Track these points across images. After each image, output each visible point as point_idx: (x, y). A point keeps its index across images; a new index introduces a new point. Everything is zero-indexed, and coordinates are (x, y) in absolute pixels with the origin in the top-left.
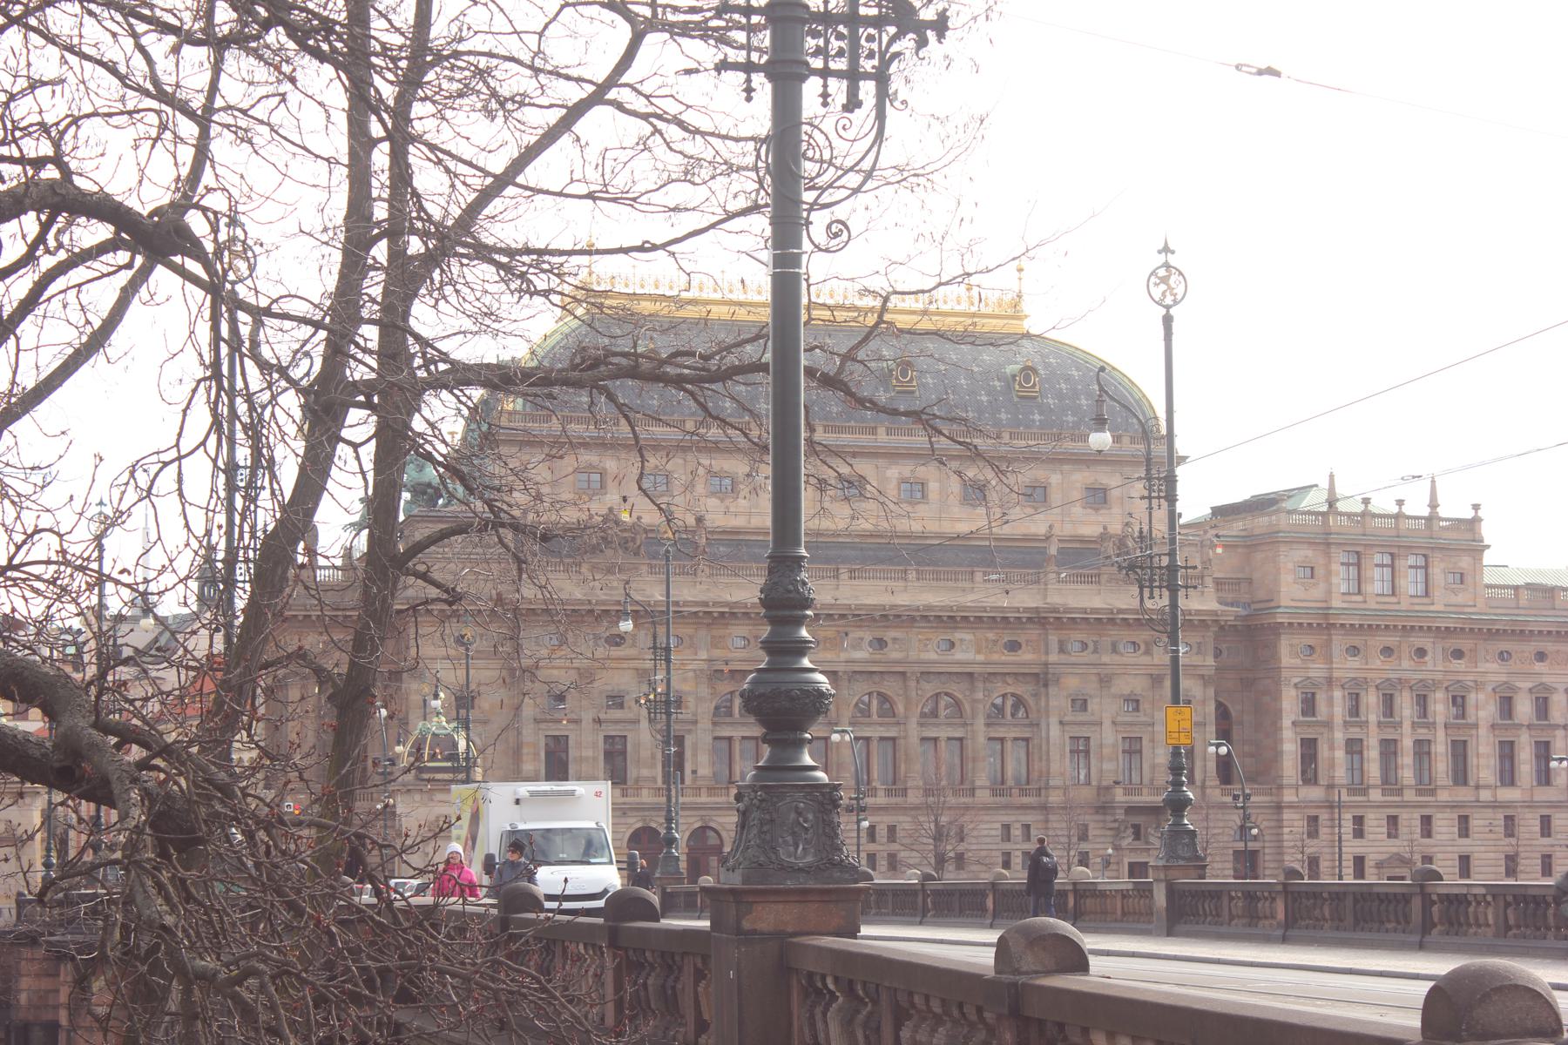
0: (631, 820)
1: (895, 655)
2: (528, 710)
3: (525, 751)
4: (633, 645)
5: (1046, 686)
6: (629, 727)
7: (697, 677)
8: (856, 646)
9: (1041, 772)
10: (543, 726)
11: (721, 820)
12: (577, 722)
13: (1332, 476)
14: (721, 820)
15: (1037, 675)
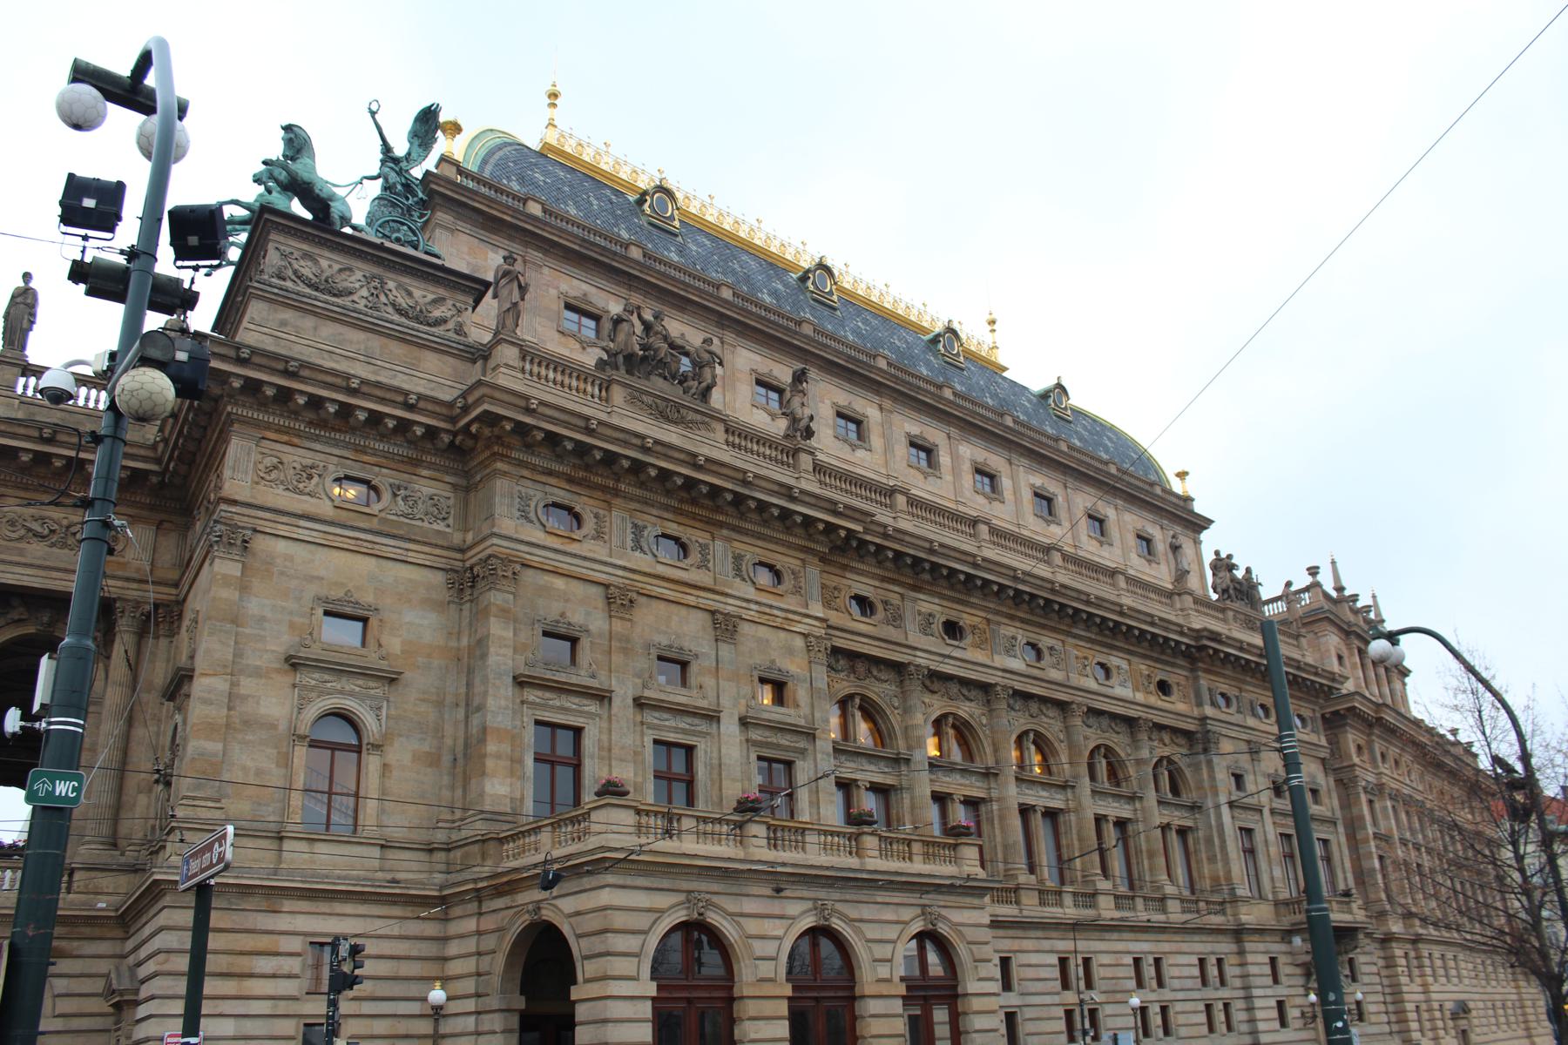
0: (793, 908)
1: (1055, 675)
2: (502, 658)
3: (491, 747)
4: (703, 565)
5: (1206, 750)
6: (703, 726)
7: (809, 648)
8: (1009, 651)
9: (1215, 880)
10: (532, 695)
11: (957, 916)
12: (602, 697)
13: (1333, 563)
14: (957, 916)
15: (1187, 734)
